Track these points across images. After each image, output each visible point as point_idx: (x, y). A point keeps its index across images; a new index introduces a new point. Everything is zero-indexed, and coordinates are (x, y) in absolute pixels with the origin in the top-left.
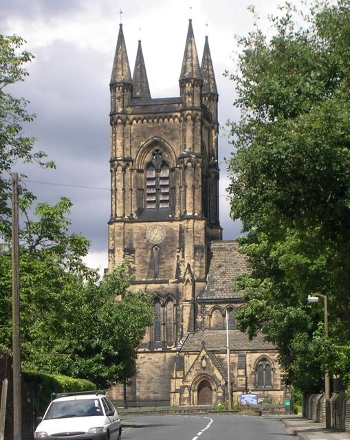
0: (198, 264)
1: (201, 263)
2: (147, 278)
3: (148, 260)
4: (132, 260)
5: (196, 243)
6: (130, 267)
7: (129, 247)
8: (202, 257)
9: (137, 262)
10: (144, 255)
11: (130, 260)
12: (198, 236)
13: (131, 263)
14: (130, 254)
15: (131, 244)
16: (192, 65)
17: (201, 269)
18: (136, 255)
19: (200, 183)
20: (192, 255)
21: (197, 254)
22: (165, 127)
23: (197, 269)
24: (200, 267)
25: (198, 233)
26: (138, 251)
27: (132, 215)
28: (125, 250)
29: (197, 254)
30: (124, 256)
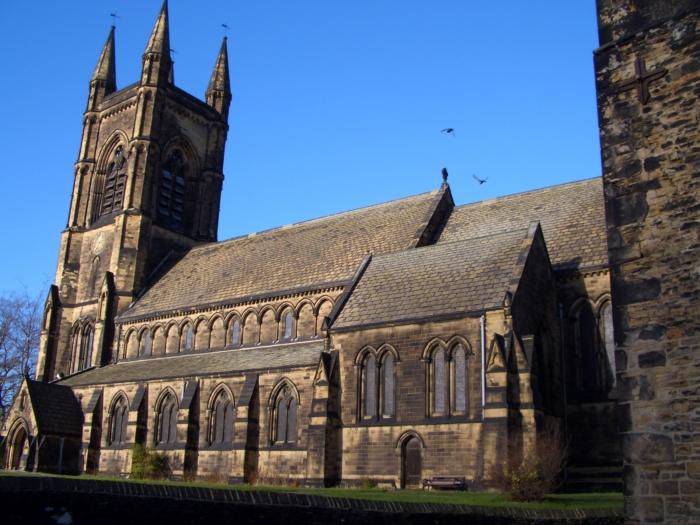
0: (123, 272)
1: (128, 271)
2: (86, 298)
3: (88, 276)
5: (126, 245)
6: (69, 286)
8: (131, 263)
12: (130, 235)
14: (72, 271)
15: (77, 259)
16: (154, 40)
17: (128, 279)
19: (144, 171)
20: (117, 261)
21: (124, 259)
22: (126, 116)
23: (121, 278)
24: (127, 276)
26: (82, 266)
27: (85, 224)
29: (124, 259)
30: (64, 273)
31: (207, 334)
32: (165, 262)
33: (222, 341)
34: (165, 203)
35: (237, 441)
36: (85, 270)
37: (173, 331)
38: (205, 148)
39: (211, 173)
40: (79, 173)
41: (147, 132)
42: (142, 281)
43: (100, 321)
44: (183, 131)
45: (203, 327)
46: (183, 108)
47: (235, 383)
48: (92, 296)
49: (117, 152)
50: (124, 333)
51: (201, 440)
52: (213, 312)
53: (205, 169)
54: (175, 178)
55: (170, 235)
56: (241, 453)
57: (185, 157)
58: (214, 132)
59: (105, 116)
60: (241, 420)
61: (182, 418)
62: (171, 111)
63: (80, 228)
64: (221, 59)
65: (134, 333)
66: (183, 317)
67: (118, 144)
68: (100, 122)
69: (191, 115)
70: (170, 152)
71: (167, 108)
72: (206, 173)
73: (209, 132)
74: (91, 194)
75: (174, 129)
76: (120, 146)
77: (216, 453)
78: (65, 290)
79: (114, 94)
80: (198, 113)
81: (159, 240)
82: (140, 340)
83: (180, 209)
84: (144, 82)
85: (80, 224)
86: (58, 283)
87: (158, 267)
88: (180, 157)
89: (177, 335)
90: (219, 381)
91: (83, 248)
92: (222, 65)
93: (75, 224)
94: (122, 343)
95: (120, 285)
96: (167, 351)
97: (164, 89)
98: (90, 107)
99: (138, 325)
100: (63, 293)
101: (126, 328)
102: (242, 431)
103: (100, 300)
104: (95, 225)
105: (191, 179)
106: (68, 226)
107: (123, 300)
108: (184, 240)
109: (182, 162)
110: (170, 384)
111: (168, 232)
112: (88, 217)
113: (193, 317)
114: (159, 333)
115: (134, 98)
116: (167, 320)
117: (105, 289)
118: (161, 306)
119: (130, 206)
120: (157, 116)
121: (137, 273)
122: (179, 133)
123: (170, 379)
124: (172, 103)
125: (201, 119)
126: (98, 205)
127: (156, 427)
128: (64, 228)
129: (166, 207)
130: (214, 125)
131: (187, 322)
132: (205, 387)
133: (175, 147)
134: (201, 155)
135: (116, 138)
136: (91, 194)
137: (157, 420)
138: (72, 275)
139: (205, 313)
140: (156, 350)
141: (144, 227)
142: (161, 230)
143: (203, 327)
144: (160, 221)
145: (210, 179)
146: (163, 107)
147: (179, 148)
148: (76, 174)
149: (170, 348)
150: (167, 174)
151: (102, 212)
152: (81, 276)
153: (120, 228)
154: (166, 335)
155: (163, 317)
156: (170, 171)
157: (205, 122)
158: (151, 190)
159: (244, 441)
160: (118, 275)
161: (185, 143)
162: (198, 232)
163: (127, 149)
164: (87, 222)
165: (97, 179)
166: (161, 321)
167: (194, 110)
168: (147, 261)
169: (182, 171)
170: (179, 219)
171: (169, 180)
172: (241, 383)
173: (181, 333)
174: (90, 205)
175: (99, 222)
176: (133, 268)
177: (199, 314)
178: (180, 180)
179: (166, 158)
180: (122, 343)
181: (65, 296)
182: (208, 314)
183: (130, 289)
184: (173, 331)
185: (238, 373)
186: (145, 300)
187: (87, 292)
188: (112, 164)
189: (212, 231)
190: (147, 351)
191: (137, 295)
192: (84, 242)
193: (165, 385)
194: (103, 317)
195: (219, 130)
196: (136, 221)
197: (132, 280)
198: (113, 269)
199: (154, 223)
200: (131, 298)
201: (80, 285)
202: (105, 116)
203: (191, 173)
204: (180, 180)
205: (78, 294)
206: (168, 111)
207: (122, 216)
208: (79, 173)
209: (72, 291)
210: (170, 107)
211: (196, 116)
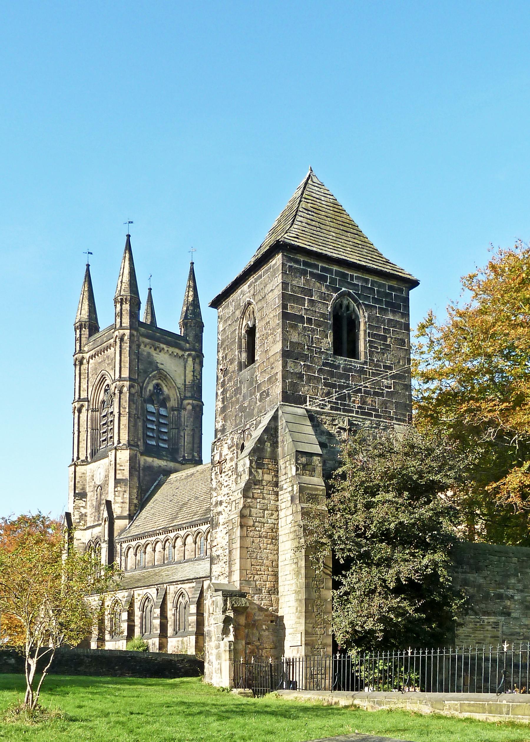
0: (119, 499)
1: (123, 498)
3: (94, 503)
4: (84, 505)
5: (118, 477)
7: (82, 491)
8: (125, 491)
9: (88, 507)
10: (92, 498)
11: (80, 505)
12: (121, 468)
13: (82, 508)
17: (124, 505)
18: (88, 499)
19: (127, 410)
21: (119, 489)
24: (123, 503)
25: (120, 466)
26: (89, 494)
27: (87, 457)
28: (75, 495)
30: (74, 501)
31: (183, 548)
32: (155, 486)
33: (193, 553)
34: (151, 434)
35: (190, 629)
36: (92, 498)
37: (159, 546)
38: (183, 378)
39: (191, 401)
40: (76, 411)
41: (126, 374)
42: (136, 506)
43: (105, 541)
44: (160, 366)
45: (179, 542)
46: (157, 344)
47: (189, 588)
48: (99, 520)
49: (106, 390)
50: (123, 550)
51: (170, 631)
52: (185, 531)
53: (186, 398)
54: (158, 410)
55: (157, 462)
56: (193, 638)
57: (165, 389)
58: (190, 360)
59: (92, 357)
60: (191, 614)
61: (155, 615)
62: (147, 349)
63: (83, 461)
64: (189, 286)
65: (131, 550)
66: (164, 536)
67: (105, 384)
68: (88, 363)
69: (166, 349)
70: (151, 387)
71: (142, 347)
72: (186, 402)
73: (186, 362)
74: (89, 430)
75: (152, 365)
76: (108, 385)
77: (180, 639)
78: (78, 517)
79: (97, 335)
80: (172, 346)
81: (149, 468)
82: (136, 555)
83: (165, 438)
84: (118, 326)
85: (82, 457)
86: (71, 511)
87: (151, 490)
88: (160, 389)
89: (162, 551)
90: (179, 586)
91: (87, 479)
92: (191, 293)
93: (78, 458)
94: (123, 558)
95: (117, 510)
96: (156, 564)
97: (137, 330)
98: (78, 349)
99: (134, 543)
100: (75, 518)
101: (125, 545)
102: (193, 622)
103: (103, 523)
104: (95, 458)
105: (173, 409)
106: (73, 460)
107: (119, 524)
108: (172, 465)
109: (163, 394)
110: (148, 590)
111: (155, 459)
112: (89, 451)
113: (172, 535)
114: (149, 549)
115: (112, 341)
116: (153, 538)
117: (106, 515)
118: (149, 528)
119: (119, 442)
120: (134, 357)
121: (130, 499)
122: (157, 368)
123: (148, 586)
124: (147, 341)
125: (177, 351)
126: (96, 440)
127: (141, 623)
128: (70, 462)
129: (153, 437)
130: (189, 355)
131: (168, 539)
132: (171, 592)
133: (155, 382)
134: (179, 386)
135: (103, 379)
136: (89, 430)
137: (142, 618)
138: (81, 503)
139: (180, 532)
140: (148, 563)
141: (132, 459)
142: (149, 459)
143: (179, 542)
144: (149, 451)
145: (189, 407)
146: (139, 346)
147: (159, 381)
148: (74, 412)
149: (158, 561)
150: (151, 408)
151: (100, 446)
152: (88, 503)
153: (113, 462)
154: (154, 550)
155: (150, 536)
156: (153, 404)
157: (180, 353)
158: (135, 425)
159: (195, 629)
160: (116, 502)
161: (163, 375)
162: (184, 456)
163: (112, 387)
164: (88, 456)
165: (92, 416)
166: (149, 539)
167: (168, 344)
168: (140, 488)
169: (163, 403)
170: (166, 446)
171: (154, 413)
172: (193, 587)
173: (164, 549)
174: (89, 441)
175: (98, 455)
176: (127, 495)
177: (175, 533)
178: (163, 411)
179: (148, 393)
180: (123, 558)
181: (78, 521)
182: (182, 533)
183: (126, 513)
184: (159, 546)
185: (190, 581)
186: (136, 523)
187: (95, 516)
188: (103, 402)
189: (196, 454)
190: (142, 564)
191: (131, 517)
192: (88, 474)
193: (145, 591)
194: (107, 538)
195: (194, 359)
196: (124, 456)
197: (127, 506)
198: (110, 498)
199: (142, 454)
200: (128, 521)
201: (89, 511)
202: (92, 357)
203: (173, 403)
204: (163, 411)
205: (88, 519)
206: (145, 350)
207: (114, 451)
208: (76, 411)
209: (83, 516)
210: (145, 346)
211: (171, 349)
